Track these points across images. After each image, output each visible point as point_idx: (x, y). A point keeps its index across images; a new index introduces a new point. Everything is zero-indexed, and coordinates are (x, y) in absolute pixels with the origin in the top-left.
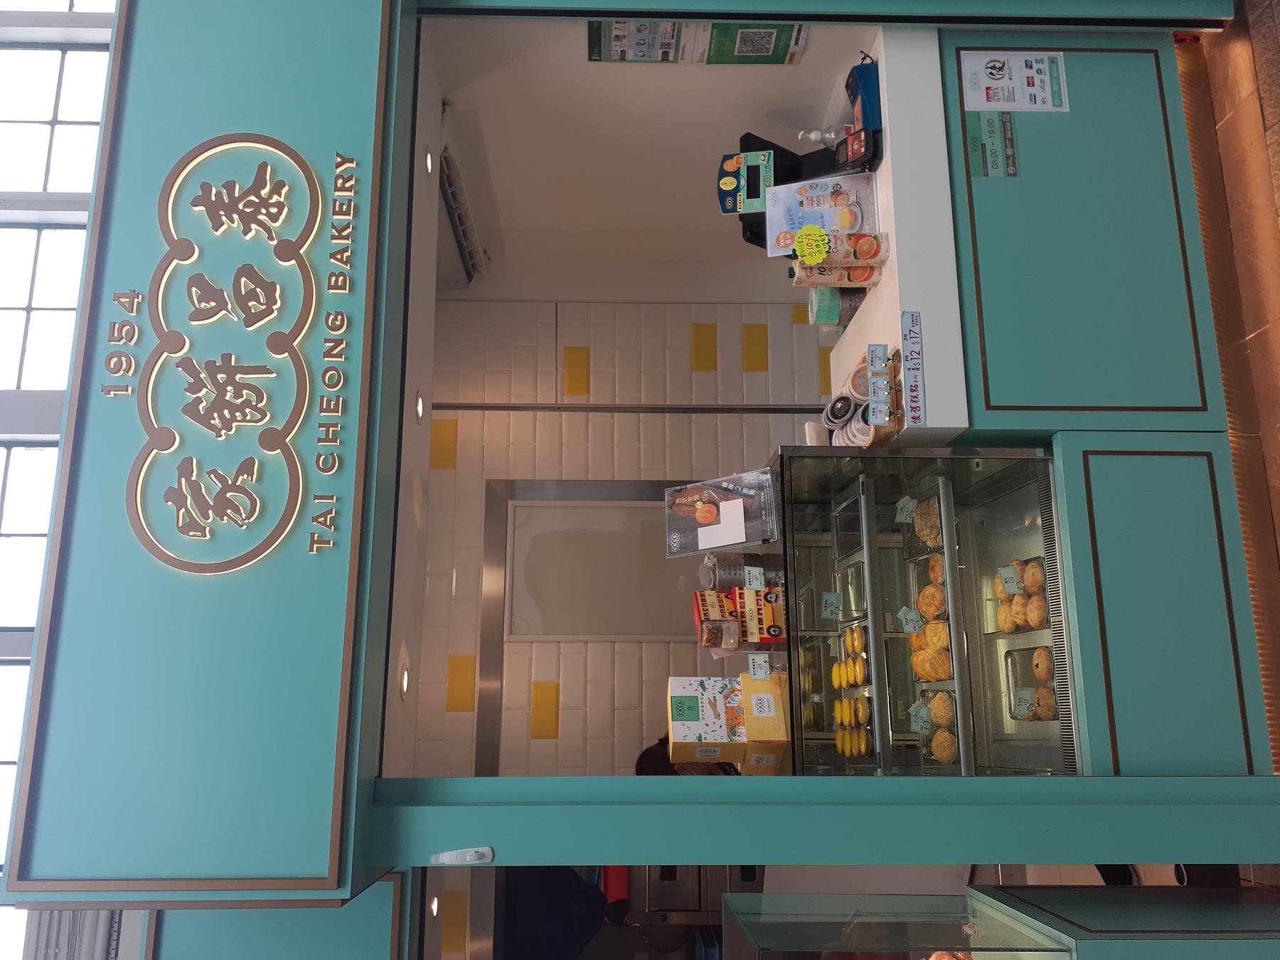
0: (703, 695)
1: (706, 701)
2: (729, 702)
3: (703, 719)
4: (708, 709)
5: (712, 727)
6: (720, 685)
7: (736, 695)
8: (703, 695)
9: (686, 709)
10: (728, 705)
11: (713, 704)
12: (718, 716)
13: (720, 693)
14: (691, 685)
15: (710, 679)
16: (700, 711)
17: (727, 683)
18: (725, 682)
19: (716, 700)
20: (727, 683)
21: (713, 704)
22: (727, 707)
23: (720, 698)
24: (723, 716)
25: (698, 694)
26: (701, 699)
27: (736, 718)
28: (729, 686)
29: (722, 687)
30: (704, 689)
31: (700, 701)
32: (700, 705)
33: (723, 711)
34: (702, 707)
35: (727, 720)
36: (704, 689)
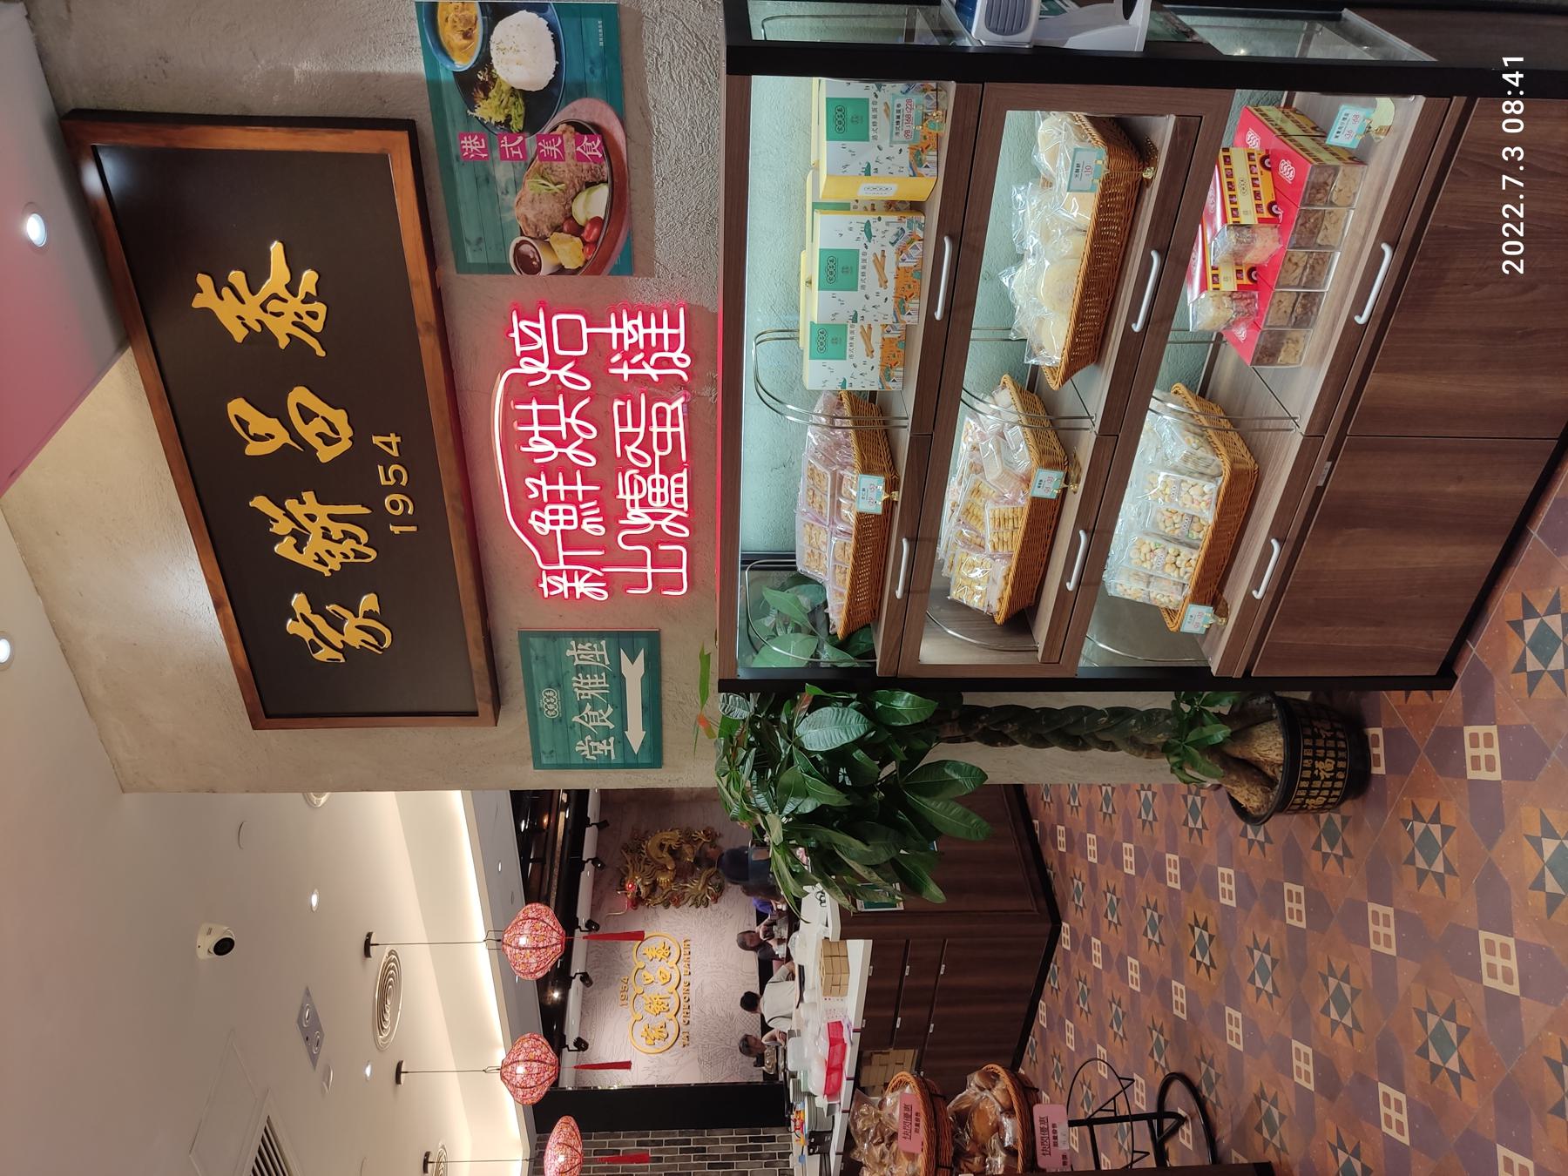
0: (866, 247)
1: (870, 258)
2: (903, 260)
3: (863, 287)
4: (872, 273)
5: (862, 368)
6: (893, 230)
7: (915, 247)
8: (866, 247)
9: (840, 270)
10: (901, 265)
11: (880, 264)
12: (884, 283)
13: (893, 244)
14: (851, 229)
15: (880, 219)
16: (860, 274)
17: (905, 227)
18: (901, 225)
19: (883, 256)
20: (905, 227)
21: (880, 264)
22: (898, 268)
23: (891, 252)
24: (892, 283)
25: (859, 246)
26: (865, 254)
27: (909, 287)
28: (907, 233)
29: (897, 234)
30: (870, 236)
31: (861, 256)
32: (861, 264)
33: (893, 276)
34: (864, 267)
35: (897, 289)
36: (870, 236)
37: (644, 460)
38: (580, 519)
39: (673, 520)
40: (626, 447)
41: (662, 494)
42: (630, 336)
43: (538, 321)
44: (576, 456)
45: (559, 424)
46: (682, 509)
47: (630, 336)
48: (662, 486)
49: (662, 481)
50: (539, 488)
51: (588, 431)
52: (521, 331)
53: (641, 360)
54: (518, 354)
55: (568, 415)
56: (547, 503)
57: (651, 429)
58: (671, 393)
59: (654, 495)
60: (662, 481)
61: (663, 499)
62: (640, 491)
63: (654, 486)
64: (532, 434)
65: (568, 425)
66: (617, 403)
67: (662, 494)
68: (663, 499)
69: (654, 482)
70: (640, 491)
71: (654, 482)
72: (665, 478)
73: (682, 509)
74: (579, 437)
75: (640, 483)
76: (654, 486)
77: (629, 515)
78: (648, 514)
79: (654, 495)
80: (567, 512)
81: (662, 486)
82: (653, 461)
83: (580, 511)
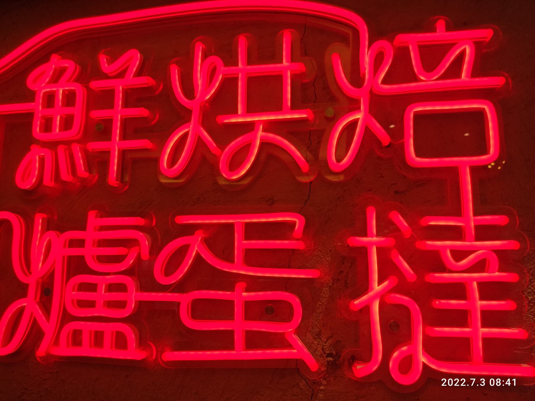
37: (168, 271)
38: (53, 145)
39: (35, 325)
40: (199, 236)
41: (91, 304)
42: (459, 254)
43: (474, 73)
44: (183, 139)
45: (249, 110)
46: (56, 342)
47: (459, 254)
48: (111, 304)
49: (122, 305)
50: (121, 75)
51: (235, 165)
52: (448, 47)
53: (397, 270)
54: (401, 39)
55: (269, 126)
56: (87, 88)
57: (240, 285)
58: (319, 335)
59: (92, 287)
60: (122, 305)
61: (82, 304)
62: (102, 259)
63: (111, 288)
64: (231, 60)
65: (251, 127)
66: (297, 221)
67: (91, 304)
68: (82, 304)
69: (121, 288)
70: (102, 259)
71: (121, 288)
72: (125, 313)
73: (56, 342)
74: (222, 146)
75: (119, 259)
76: (111, 288)
77: (52, 235)
78: (51, 276)
79: (92, 287)
80: (67, 123)
81: (111, 304)
82: (164, 288)
83: (68, 143)
